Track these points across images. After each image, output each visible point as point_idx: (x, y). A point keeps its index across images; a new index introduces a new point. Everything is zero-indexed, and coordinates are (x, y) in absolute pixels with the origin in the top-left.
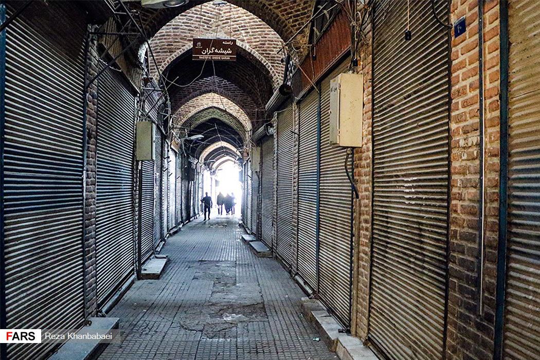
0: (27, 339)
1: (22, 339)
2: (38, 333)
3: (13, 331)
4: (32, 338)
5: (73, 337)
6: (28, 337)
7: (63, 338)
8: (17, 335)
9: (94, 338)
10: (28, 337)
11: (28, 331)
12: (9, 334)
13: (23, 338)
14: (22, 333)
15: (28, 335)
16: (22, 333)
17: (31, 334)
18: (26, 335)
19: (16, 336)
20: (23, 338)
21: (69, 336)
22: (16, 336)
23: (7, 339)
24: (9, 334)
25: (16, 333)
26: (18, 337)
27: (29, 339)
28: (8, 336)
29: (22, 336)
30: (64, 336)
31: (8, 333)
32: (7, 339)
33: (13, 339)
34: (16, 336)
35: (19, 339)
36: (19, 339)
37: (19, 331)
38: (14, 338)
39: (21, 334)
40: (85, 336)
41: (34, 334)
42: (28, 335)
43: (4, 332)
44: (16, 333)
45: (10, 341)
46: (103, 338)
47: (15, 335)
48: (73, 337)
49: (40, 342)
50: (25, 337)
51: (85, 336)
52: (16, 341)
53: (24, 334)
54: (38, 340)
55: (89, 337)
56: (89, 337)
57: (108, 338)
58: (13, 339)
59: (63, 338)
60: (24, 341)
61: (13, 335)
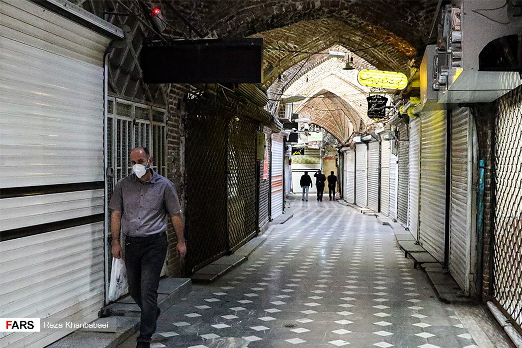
0: (26, 328)
1: (21, 328)
4: (31, 327)
5: (70, 326)
6: (27, 325)
8: (17, 324)
10: (27, 325)
12: (9, 323)
14: (21, 322)
15: (27, 324)
16: (21, 322)
17: (30, 323)
18: (26, 324)
19: (15, 325)
22: (15, 325)
23: (7, 328)
24: (9, 323)
25: (15, 322)
26: (17, 326)
27: (28, 327)
28: (7, 325)
29: (21, 325)
31: (7, 322)
32: (7, 328)
33: (13, 328)
35: (18, 328)
36: (18, 328)
38: (14, 326)
39: (21, 323)
40: (82, 325)
41: (33, 322)
42: (27, 324)
44: (15, 322)
46: (100, 326)
47: (14, 324)
48: (70, 326)
50: (24, 325)
51: (82, 325)
53: (23, 323)
57: (104, 326)
58: (13, 328)
61: (12, 323)
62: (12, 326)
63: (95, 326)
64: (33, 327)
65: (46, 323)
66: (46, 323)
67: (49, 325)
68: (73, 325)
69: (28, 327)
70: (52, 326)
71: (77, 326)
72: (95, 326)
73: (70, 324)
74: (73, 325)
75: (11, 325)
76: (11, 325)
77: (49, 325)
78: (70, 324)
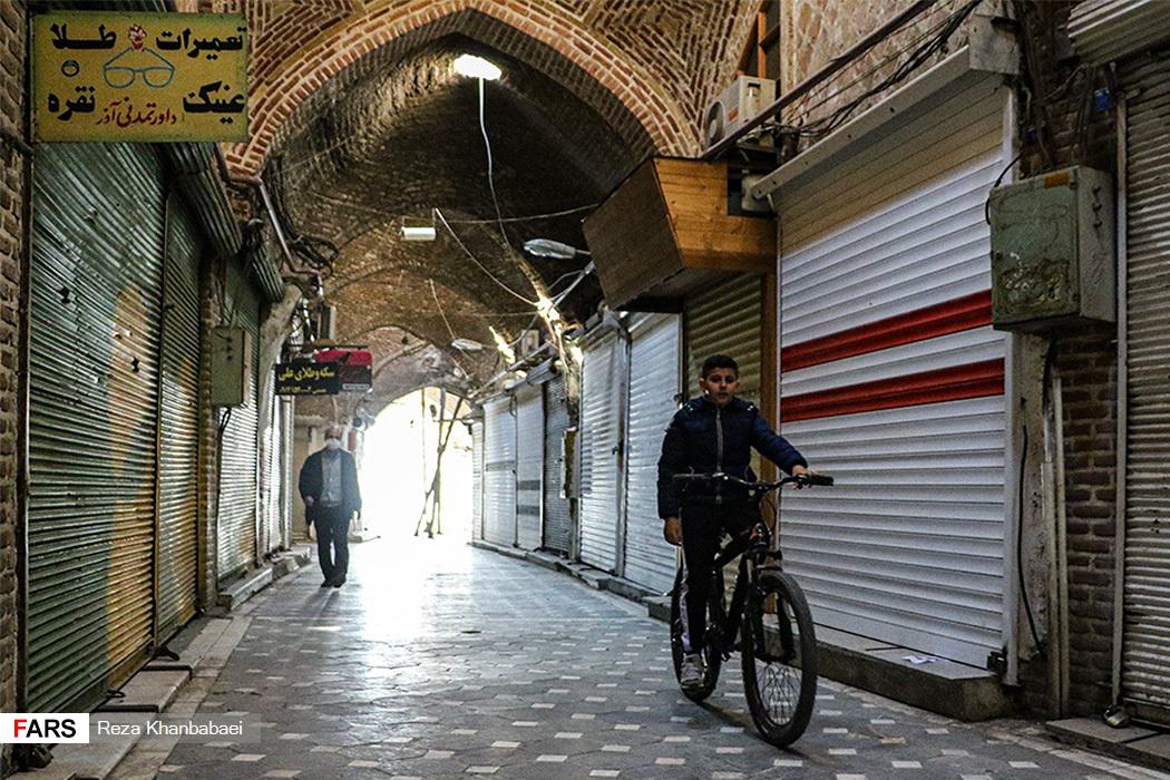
0: (58, 735)
1: (47, 735)
2: (82, 720)
3: (29, 717)
4: (69, 732)
5: (158, 730)
6: (60, 729)
7: (135, 732)
8: (37, 727)
10: (60, 729)
11: (61, 717)
12: (20, 724)
13: (50, 732)
14: (47, 721)
15: (61, 726)
16: (47, 721)
17: (68, 724)
18: (57, 726)
19: (34, 728)
20: (50, 732)
21: (149, 728)
22: (34, 728)
23: (16, 735)
24: (20, 724)
25: (34, 722)
26: (38, 731)
27: (64, 734)
28: (17, 728)
29: (47, 728)
31: (16, 722)
32: (16, 735)
33: (28, 735)
34: (34, 728)
35: (41, 736)
36: (41, 736)
37: (41, 718)
38: (30, 731)
39: (47, 725)
41: (73, 723)
42: (61, 726)
43: (8, 719)
44: (34, 722)
45: (22, 739)
47: (32, 726)
48: (158, 730)
49: (86, 740)
50: (54, 729)
52: (35, 739)
53: (52, 725)
55: (194, 729)
58: (28, 735)
59: (135, 732)
60: (52, 739)
61: (28, 725)
62: (27, 730)
63: (214, 730)
65: (104, 725)
66: (103, 725)
67: (110, 729)
70: (115, 732)
71: (173, 731)
72: (214, 730)
77: (110, 729)
78: (157, 727)
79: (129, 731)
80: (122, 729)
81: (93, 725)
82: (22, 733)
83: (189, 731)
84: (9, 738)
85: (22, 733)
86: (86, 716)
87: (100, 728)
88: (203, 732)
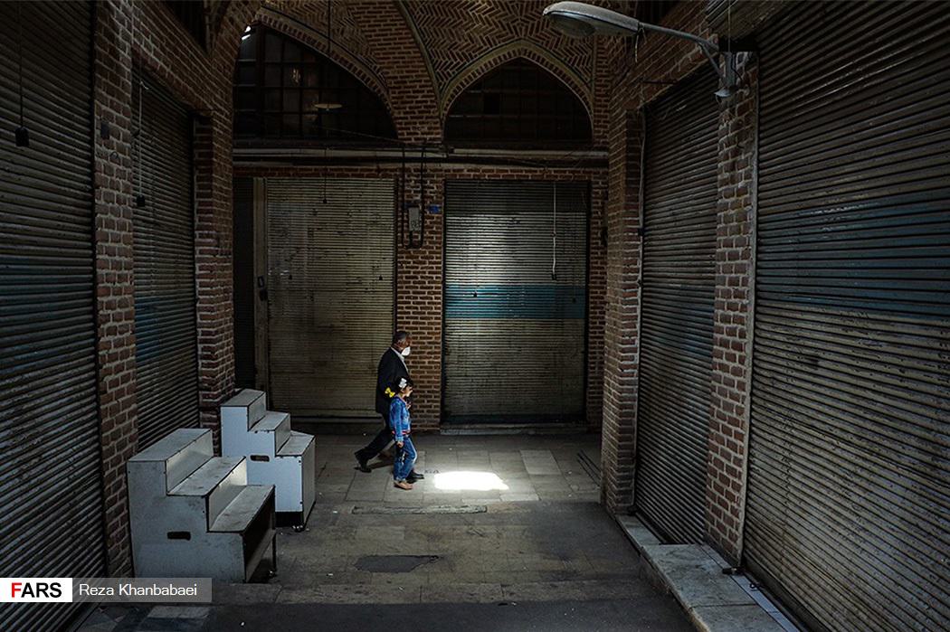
0: (47, 596)
1: (38, 596)
2: (67, 584)
3: (24, 581)
4: (56, 593)
6: (49, 591)
7: (110, 593)
8: (30, 589)
9: (165, 593)
10: (49, 591)
11: (49, 581)
12: (16, 587)
13: (41, 593)
14: (38, 585)
16: (38, 585)
17: (55, 586)
18: (47, 588)
19: (28, 590)
20: (41, 593)
21: (121, 590)
22: (28, 590)
23: (13, 595)
24: (16, 587)
25: (28, 585)
26: (31, 593)
27: (52, 594)
28: (14, 590)
29: (38, 590)
30: (112, 591)
31: (13, 585)
32: (13, 595)
33: (23, 596)
34: (28, 590)
35: (33, 596)
36: (33, 596)
37: (33, 581)
38: (25, 593)
43: (9, 581)
44: (28, 585)
45: (18, 599)
46: (182, 593)
47: (26, 588)
49: (70, 600)
50: (43, 591)
52: (28, 599)
53: (42, 587)
54: (67, 597)
55: (157, 591)
56: (157, 591)
57: (190, 593)
58: (23, 596)
59: (110, 593)
60: (42, 599)
61: (22, 587)
62: (21, 593)
63: (174, 591)
64: (60, 593)
65: (85, 588)
67: (89, 591)
68: (133, 591)
69: (52, 594)
70: (94, 593)
71: (141, 593)
72: (174, 591)
73: (127, 589)
74: (133, 591)
75: (19, 590)
76: (19, 590)
77: (89, 591)
78: (127, 589)
79: (105, 592)
80: (99, 590)
81: (75, 590)
82: (18, 594)
83: (153, 592)
84: (7, 598)
85: (18, 594)
86: (70, 580)
87: (81, 590)
88: (165, 593)
